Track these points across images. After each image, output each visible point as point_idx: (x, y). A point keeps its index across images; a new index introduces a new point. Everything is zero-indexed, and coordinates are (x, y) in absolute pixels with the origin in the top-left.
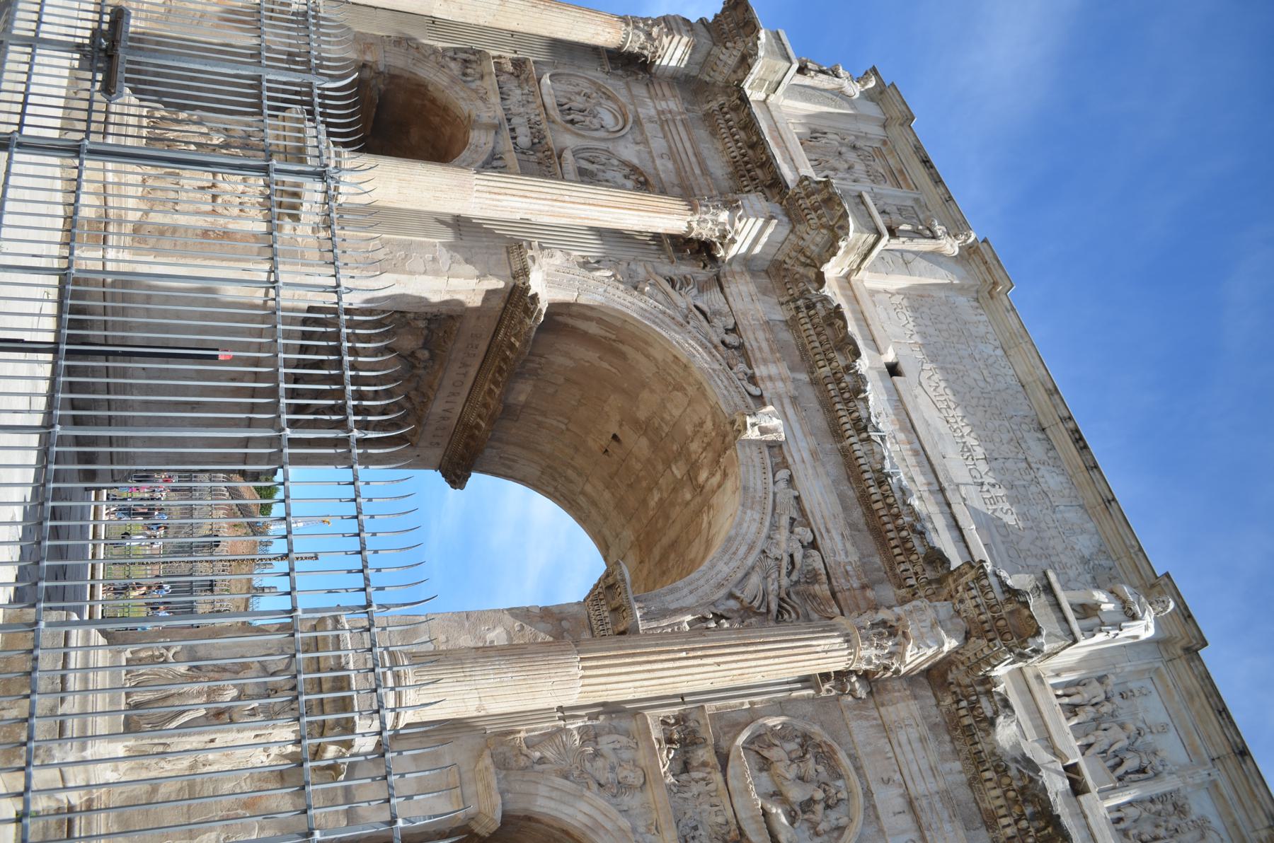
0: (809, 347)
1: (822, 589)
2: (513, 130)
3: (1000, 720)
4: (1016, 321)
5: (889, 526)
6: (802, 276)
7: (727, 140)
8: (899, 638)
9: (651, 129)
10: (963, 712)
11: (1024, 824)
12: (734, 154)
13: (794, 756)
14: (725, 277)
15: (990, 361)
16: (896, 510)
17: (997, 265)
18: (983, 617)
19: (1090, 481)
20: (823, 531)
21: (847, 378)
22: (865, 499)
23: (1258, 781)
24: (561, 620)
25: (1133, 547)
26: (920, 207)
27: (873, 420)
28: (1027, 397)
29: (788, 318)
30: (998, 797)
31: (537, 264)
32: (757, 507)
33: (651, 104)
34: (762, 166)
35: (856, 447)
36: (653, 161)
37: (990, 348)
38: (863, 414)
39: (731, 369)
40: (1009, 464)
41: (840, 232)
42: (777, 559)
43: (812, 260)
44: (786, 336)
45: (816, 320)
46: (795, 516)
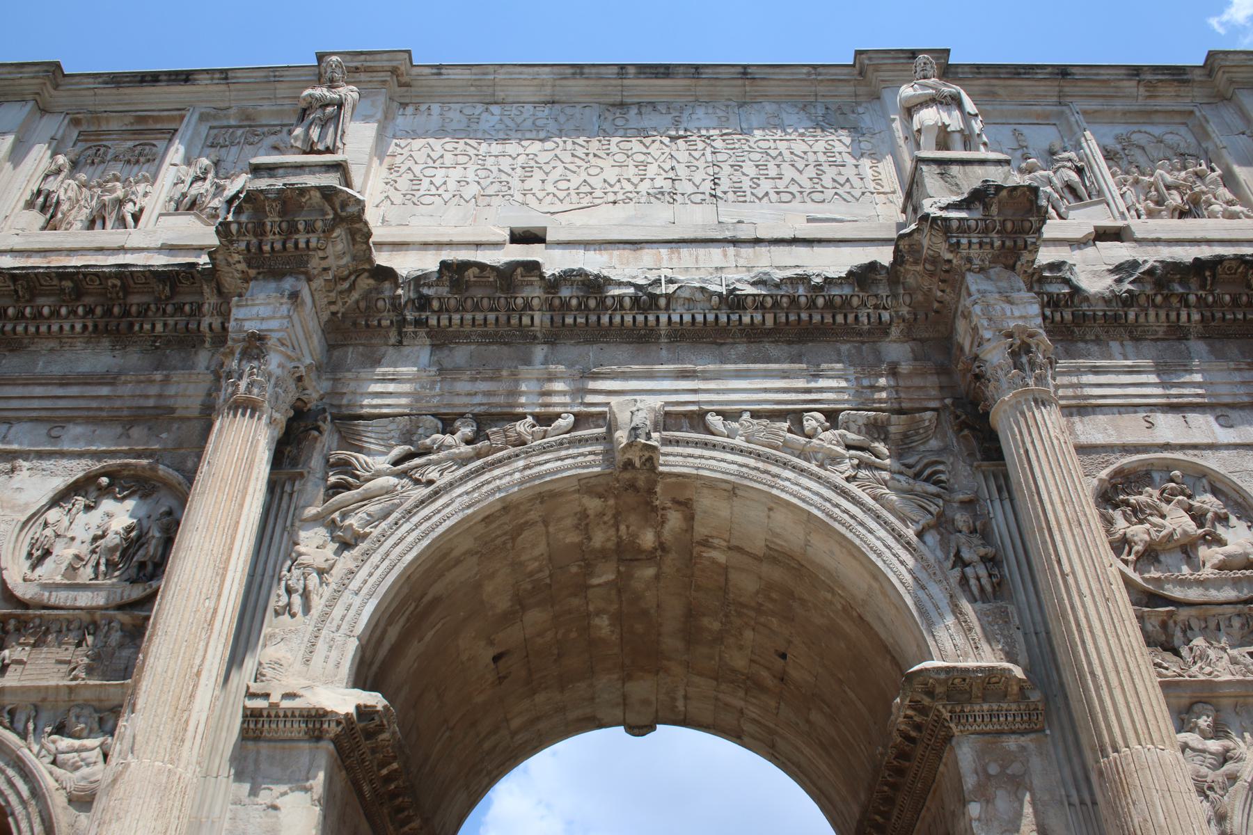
0: (491, 328)
1: (897, 425)
4: (458, 71)
5: (804, 316)
6: (366, 296)
7: (43, 329)
8: (1032, 341)
10: (1058, 317)
11: (1192, 298)
12: (78, 327)
13: (1134, 519)
14: (340, 406)
16: (785, 300)
17: (368, 58)
18: (997, 243)
19: (713, 82)
21: (565, 292)
22: (754, 334)
23: (1094, 71)
24: (989, 777)
25: (809, 74)
26: (215, 117)
28: (573, 104)
29: (428, 341)
30: (1157, 314)
31: (301, 692)
32: (774, 469)
34: (126, 290)
35: (676, 318)
37: (485, 115)
38: (631, 290)
41: (352, 209)
42: (858, 466)
43: (355, 271)
44: (461, 354)
45: (453, 302)
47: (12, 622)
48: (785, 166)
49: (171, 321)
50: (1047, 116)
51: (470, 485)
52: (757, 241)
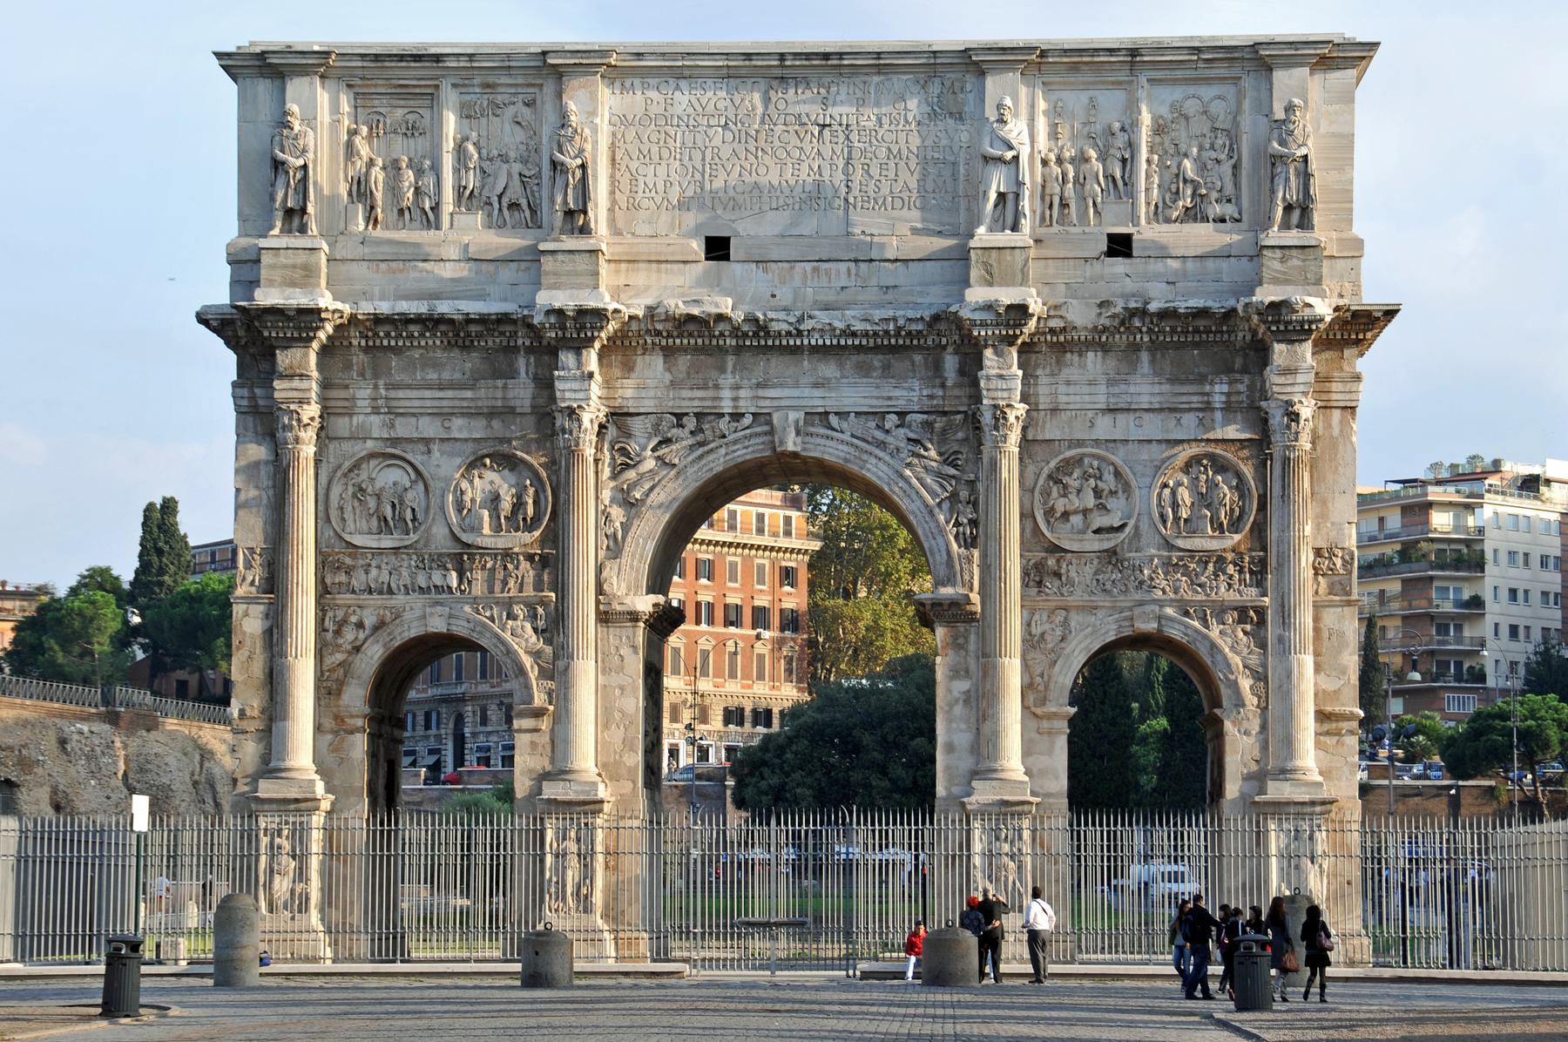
2: (436, 587)
3: (1068, 315)
7: (416, 344)
9: (403, 429)
11: (1144, 329)
12: (438, 342)
15: (700, 109)
20: (887, 403)
21: (745, 328)
22: (859, 349)
26: (464, 86)
27: (793, 320)
32: (865, 457)
33: (361, 418)
35: (813, 342)
36: (456, 439)
38: (784, 327)
39: (724, 436)
40: (827, 153)
44: (684, 361)
45: (675, 334)
46: (874, 424)
47: (465, 557)
48: (902, 164)
49: (498, 340)
50: (1120, 83)
51: (696, 467)
52: (871, 260)
